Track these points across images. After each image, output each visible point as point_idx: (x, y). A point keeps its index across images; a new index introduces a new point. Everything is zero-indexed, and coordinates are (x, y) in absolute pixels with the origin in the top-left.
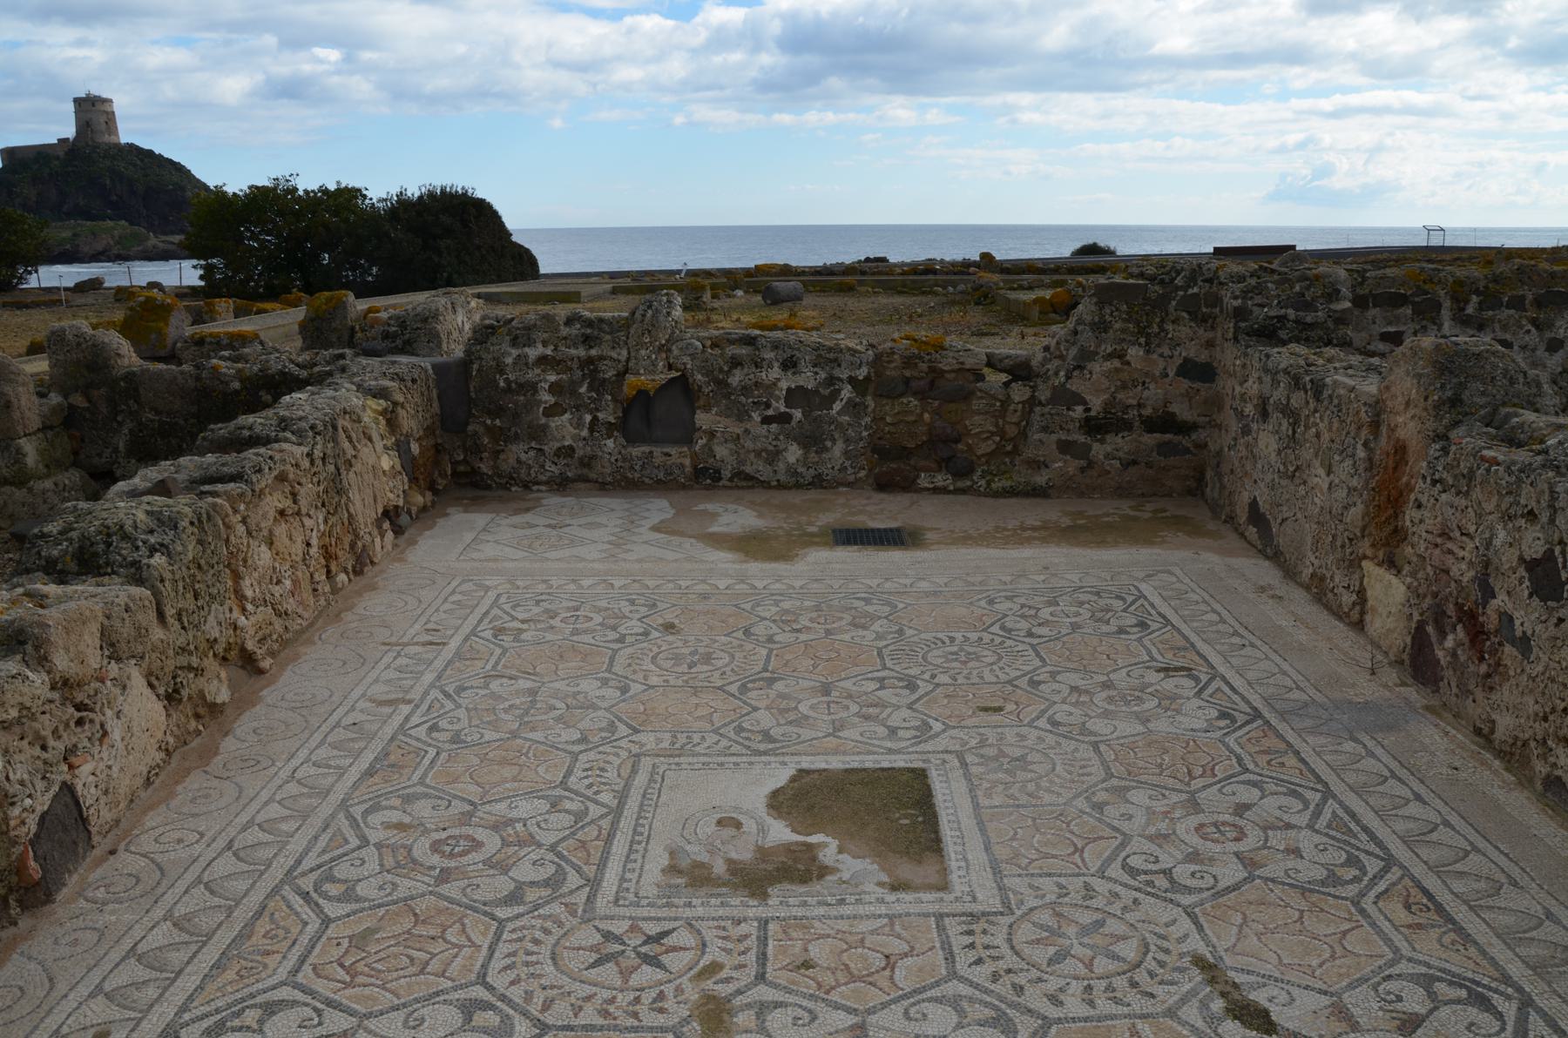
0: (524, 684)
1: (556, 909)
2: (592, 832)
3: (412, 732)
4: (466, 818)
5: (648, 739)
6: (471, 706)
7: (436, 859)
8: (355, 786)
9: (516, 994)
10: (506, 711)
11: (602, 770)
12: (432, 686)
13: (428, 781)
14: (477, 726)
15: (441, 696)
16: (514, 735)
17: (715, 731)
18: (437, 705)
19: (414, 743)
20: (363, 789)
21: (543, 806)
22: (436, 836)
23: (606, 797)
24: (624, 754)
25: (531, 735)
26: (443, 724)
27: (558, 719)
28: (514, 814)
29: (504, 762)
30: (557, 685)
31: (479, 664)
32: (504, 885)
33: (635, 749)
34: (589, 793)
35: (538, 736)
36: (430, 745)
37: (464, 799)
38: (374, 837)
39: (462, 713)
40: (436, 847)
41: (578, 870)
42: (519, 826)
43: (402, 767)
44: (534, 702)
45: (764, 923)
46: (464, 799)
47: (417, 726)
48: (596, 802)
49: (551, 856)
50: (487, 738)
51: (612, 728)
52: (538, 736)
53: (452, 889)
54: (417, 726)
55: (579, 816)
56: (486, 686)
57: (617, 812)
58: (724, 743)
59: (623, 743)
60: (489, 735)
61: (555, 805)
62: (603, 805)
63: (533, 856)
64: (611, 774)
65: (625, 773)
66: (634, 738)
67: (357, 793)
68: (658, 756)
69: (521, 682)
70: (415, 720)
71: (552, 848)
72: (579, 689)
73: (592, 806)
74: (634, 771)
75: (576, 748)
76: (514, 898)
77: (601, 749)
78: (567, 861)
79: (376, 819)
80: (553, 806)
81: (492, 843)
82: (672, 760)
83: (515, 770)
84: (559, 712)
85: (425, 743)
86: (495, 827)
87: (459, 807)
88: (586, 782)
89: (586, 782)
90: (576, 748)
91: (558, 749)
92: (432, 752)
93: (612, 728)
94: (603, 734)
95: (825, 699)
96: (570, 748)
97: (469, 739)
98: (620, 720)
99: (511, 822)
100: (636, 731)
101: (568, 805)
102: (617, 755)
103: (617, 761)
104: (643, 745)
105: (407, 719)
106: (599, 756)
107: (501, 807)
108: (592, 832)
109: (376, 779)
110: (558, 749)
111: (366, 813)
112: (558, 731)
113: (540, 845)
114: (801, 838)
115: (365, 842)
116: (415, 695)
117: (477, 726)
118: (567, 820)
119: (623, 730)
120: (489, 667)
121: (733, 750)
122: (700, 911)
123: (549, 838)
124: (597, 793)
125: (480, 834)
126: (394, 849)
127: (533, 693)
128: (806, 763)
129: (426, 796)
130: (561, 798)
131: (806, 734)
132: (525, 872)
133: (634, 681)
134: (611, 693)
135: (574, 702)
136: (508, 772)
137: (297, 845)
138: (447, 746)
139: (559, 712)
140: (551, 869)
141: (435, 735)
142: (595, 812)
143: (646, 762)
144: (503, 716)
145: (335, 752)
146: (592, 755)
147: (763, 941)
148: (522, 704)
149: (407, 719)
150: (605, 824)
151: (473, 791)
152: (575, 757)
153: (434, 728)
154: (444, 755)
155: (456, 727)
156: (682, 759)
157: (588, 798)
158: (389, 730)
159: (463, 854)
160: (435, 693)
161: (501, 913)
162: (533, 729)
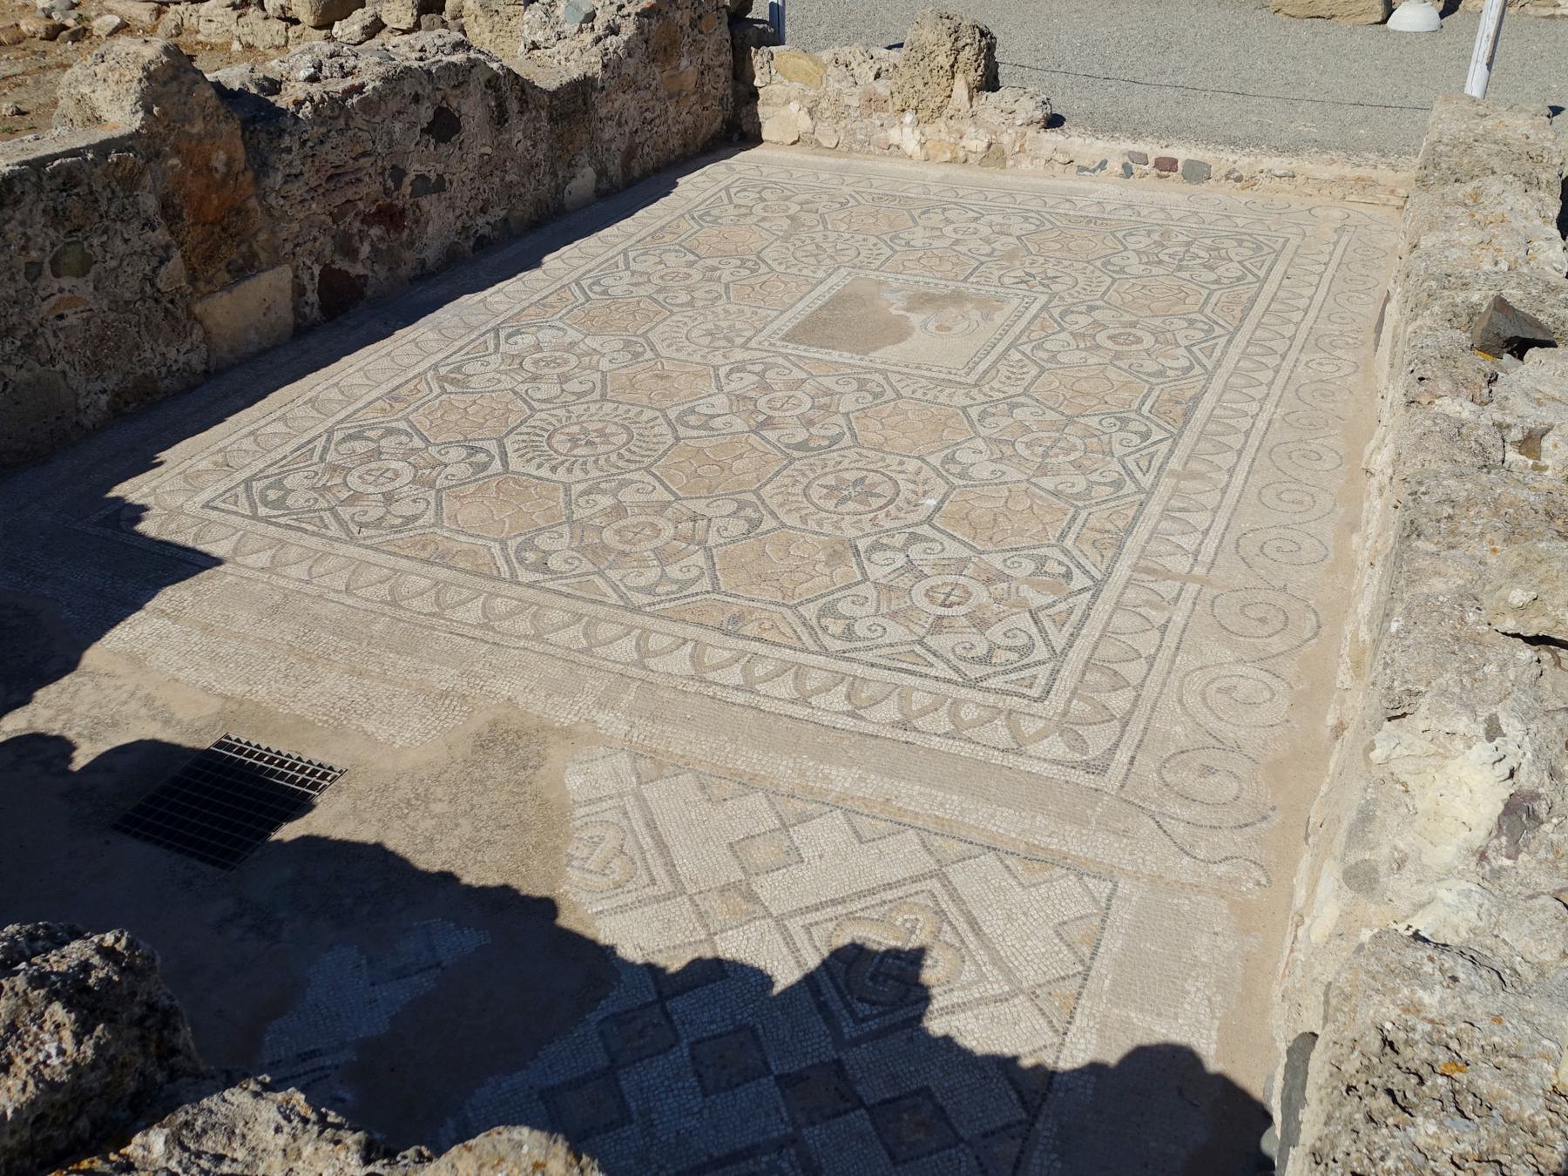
0: (1048, 482)
1: (1069, 300)
2: (1034, 336)
3: (1164, 435)
4: (1117, 356)
5: (960, 399)
6: (1108, 458)
7: (1139, 333)
8: (1204, 390)
9: (1100, 274)
10: (1073, 448)
11: (1009, 378)
12: (1150, 494)
13: (1147, 386)
14: (1104, 433)
15: (1138, 475)
16: (1071, 420)
17: (899, 396)
18: (1144, 464)
19: (1161, 422)
20: (1199, 386)
21: (1063, 358)
22: (1139, 347)
23: (1017, 356)
24: (986, 389)
25: (1058, 416)
26: (1136, 440)
27: (1028, 430)
28: (1084, 354)
29: (1084, 394)
30: (1016, 476)
31: (1093, 522)
32: (1097, 315)
33: (974, 392)
34: (1026, 361)
35: (1051, 416)
36: (1148, 418)
37: (1119, 368)
38: (1182, 351)
39: (1118, 450)
40: (1139, 340)
41: (1051, 316)
42: (1082, 345)
43: (1169, 401)
44: (1045, 455)
45: (965, 280)
46: (1119, 368)
47: (1162, 440)
48: (1024, 354)
49: (1065, 325)
50: (1097, 419)
51: (983, 416)
52: (1051, 416)
53: (1127, 318)
54: (1162, 440)
55: (1039, 347)
56: (1091, 485)
57: (1012, 345)
58: (899, 386)
59: (980, 398)
60: (1093, 422)
61: (1054, 357)
62: (1019, 351)
63: (1076, 327)
64: (1004, 371)
65: (994, 372)
66: (968, 402)
67: (1203, 383)
68: (960, 383)
69: (1051, 487)
70: (1164, 448)
71: (1063, 329)
72: (994, 466)
73: (1028, 352)
74: (986, 372)
75: (1022, 399)
76: (1091, 309)
77: (1002, 395)
78: (1056, 321)
79: (1184, 363)
80: (1054, 356)
81: (1101, 338)
82: (951, 377)
83: (1077, 387)
84: (1025, 439)
85: (1152, 421)
86: (1098, 346)
87: (1123, 364)
88: (1025, 370)
89: (1025, 370)
90: (1022, 399)
91: (1037, 401)
92: (1145, 410)
93: (983, 416)
94: (994, 410)
95: (775, 414)
96: (1028, 401)
97: (1113, 420)
98: (972, 425)
99: (1086, 349)
100: (964, 409)
101: (1045, 355)
102: (992, 389)
103: (996, 384)
104: (967, 395)
105: (1171, 452)
106: (1005, 389)
107: (1091, 361)
108: (1034, 336)
109: (1189, 394)
110: (1037, 401)
111: (1191, 368)
112: (1032, 418)
113: (1072, 333)
114: (908, 314)
115: (1188, 348)
116: (1167, 483)
117: (1104, 433)
118: (1047, 346)
119: (974, 413)
120: (1084, 514)
121: (899, 377)
122: (993, 289)
123: (1064, 336)
124: (1019, 361)
125: (1109, 344)
126: (1167, 343)
127: (1043, 470)
128: (855, 360)
129: (1149, 374)
130: (1047, 361)
131: (829, 382)
132: (1084, 320)
133: (935, 469)
134: (964, 456)
135: (1004, 450)
136: (1084, 386)
137: (1234, 353)
138: (1133, 415)
139: (1025, 439)
140: (1067, 319)
141: (1144, 429)
142: (1027, 349)
143: (971, 380)
144: (1078, 441)
145: (1232, 422)
146: (1011, 390)
147: (971, 274)
148: (1057, 455)
149: (1171, 452)
150: (1024, 339)
151: (1112, 373)
152: (1025, 393)
153: (1145, 436)
154: (1135, 406)
155: (1123, 435)
156: (942, 376)
157: (1028, 358)
158: (1187, 440)
159: (1120, 334)
160: (1146, 481)
161: (1100, 303)
162: (1053, 423)
